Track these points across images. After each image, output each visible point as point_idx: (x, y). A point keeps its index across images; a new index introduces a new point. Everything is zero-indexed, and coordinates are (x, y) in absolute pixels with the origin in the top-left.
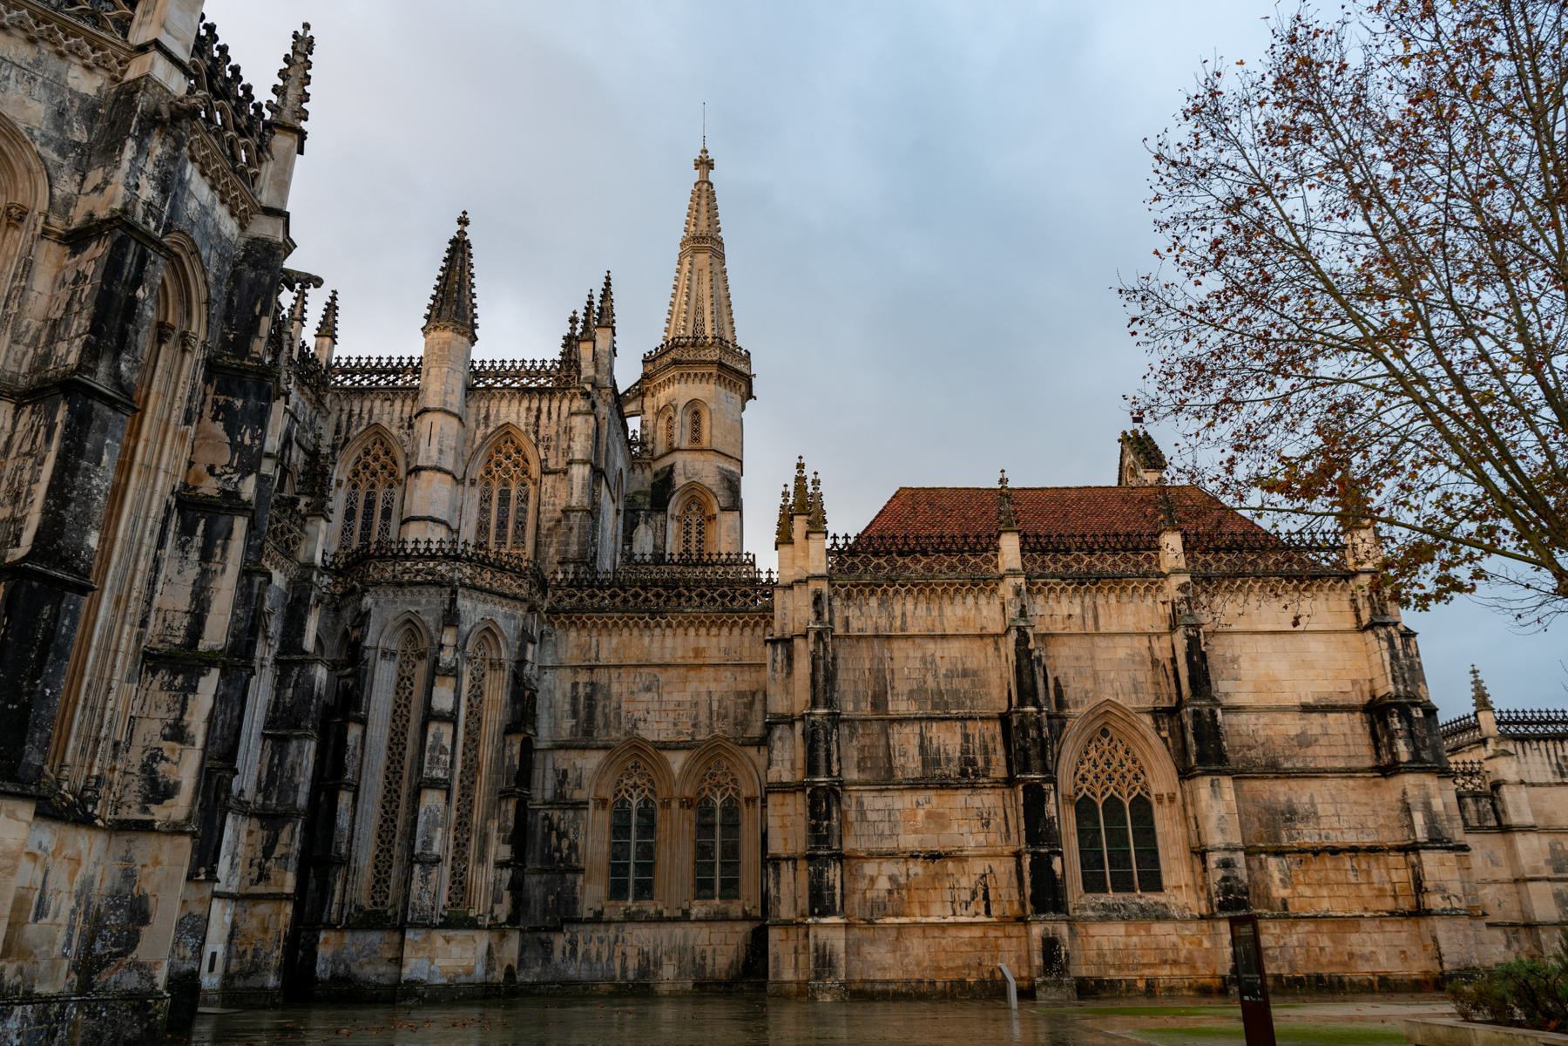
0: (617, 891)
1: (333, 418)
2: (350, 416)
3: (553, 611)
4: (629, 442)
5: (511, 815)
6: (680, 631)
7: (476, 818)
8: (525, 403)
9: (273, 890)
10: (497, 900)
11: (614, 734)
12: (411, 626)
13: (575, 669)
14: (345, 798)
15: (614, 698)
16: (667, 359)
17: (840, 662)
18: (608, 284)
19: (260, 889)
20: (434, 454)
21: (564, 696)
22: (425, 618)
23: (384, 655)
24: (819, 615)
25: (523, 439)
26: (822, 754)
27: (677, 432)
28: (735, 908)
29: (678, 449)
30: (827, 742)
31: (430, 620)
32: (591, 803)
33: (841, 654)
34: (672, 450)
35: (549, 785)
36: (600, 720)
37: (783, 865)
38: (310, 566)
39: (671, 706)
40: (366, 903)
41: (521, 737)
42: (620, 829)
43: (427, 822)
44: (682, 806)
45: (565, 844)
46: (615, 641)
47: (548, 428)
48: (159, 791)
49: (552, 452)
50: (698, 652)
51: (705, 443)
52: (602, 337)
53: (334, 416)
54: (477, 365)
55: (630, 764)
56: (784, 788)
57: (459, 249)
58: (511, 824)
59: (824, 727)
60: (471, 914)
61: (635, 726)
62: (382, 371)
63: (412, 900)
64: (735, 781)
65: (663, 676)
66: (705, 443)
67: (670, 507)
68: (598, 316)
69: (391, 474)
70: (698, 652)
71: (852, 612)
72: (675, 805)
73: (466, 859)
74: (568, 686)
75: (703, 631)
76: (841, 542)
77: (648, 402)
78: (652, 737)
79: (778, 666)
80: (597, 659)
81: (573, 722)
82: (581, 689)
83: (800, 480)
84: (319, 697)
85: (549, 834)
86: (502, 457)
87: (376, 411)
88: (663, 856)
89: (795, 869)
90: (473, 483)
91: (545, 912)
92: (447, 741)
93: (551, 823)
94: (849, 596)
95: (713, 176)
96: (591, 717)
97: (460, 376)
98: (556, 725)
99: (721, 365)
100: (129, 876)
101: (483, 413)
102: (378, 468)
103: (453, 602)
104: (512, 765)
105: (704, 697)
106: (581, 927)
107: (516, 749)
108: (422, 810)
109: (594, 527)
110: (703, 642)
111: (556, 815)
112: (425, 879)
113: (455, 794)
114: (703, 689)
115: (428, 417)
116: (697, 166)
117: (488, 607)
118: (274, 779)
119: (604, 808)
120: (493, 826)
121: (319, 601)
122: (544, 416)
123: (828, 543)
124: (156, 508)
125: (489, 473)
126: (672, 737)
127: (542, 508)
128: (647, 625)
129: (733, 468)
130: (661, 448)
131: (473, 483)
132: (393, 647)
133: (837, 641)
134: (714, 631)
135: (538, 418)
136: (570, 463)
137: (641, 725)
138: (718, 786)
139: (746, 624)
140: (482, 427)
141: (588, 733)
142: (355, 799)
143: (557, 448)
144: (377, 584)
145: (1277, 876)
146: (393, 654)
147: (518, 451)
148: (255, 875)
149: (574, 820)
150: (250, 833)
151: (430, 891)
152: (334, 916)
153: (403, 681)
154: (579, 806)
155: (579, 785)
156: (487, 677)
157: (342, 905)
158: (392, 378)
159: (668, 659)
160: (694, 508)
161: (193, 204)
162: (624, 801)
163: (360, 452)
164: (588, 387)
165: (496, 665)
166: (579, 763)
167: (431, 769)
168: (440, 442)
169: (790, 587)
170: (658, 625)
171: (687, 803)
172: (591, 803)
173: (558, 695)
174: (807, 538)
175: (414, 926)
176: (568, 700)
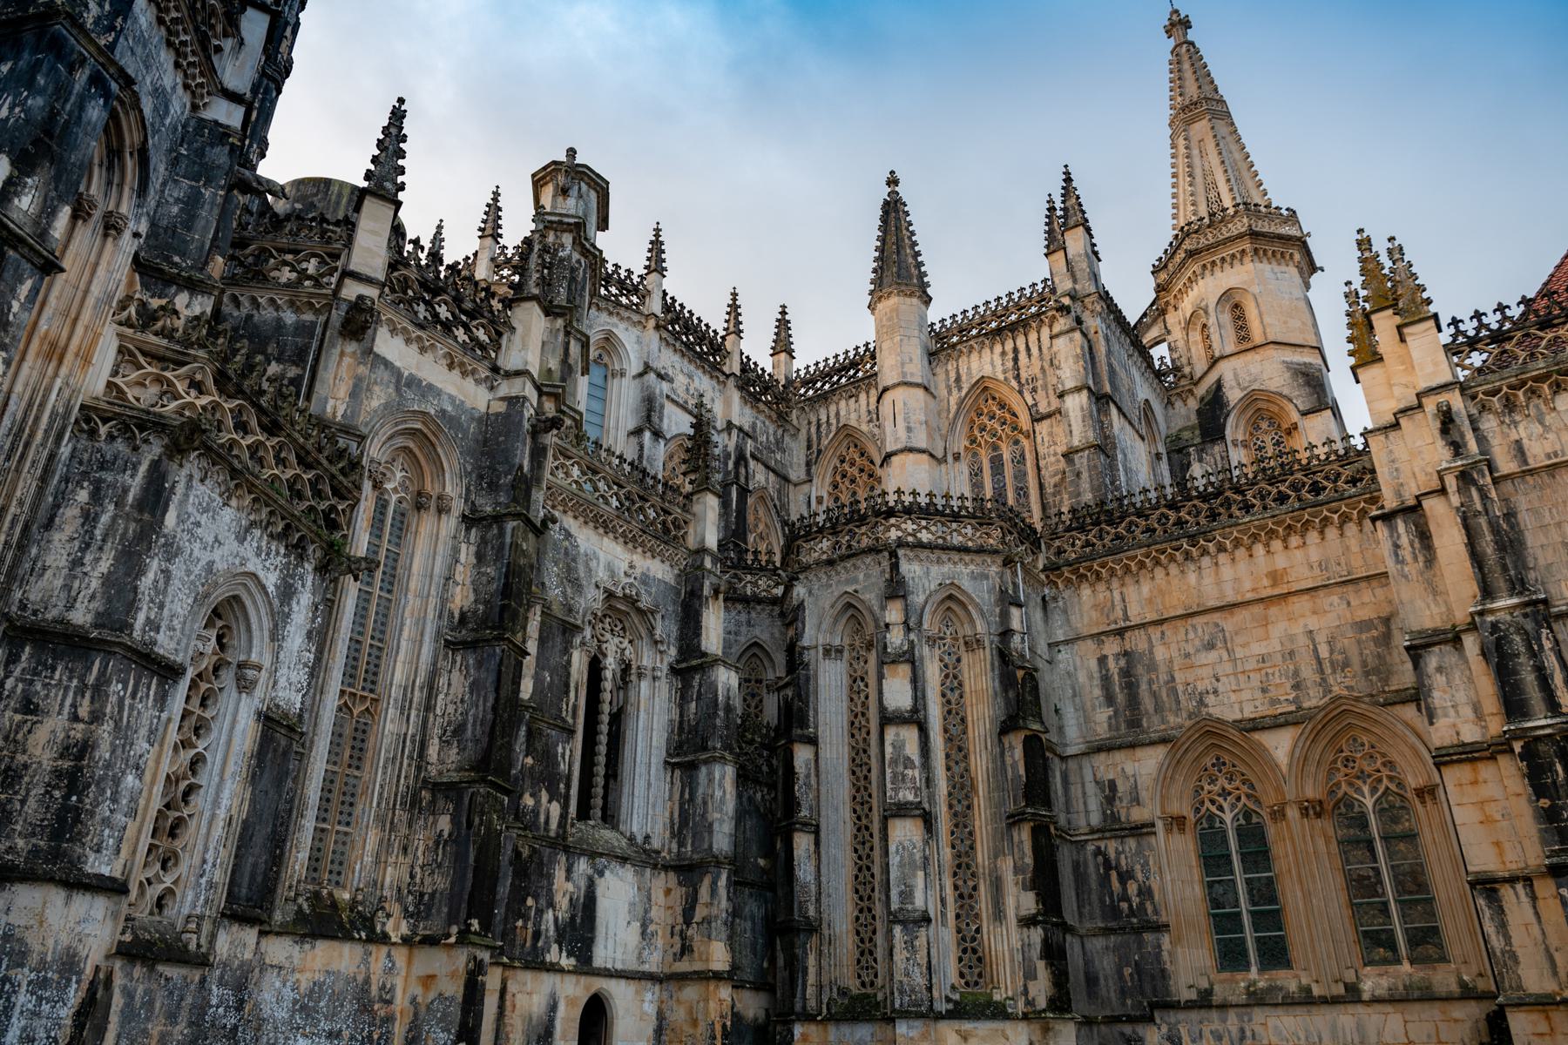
0: (1231, 957)
1: (803, 435)
2: (819, 426)
3: (1051, 568)
4: (1159, 375)
5: (1028, 847)
6: (1241, 553)
7: (982, 856)
8: (998, 348)
9: (698, 966)
10: (1030, 975)
11: (1173, 720)
12: (851, 609)
13: (1098, 637)
14: (802, 843)
15: (1163, 669)
16: (1181, 255)
17: (1525, 519)
18: (1068, 180)
19: (683, 966)
20: (902, 433)
21: (1091, 678)
22: (866, 597)
23: (827, 652)
24: (1457, 448)
25: (1004, 390)
26: (1529, 678)
27: (1215, 337)
28: (1444, 979)
29: (1222, 357)
30: (1533, 655)
31: (871, 597)
32: (1160, 825)
33: (1522, 503)
34: (1214, 362)
35: (1094, 805)
36: (1147, 703)
37: (1506, 892)
38: (702, 551)
39: (1252, 664)
40: (854, 986)
41: (1021, 735)
42: (1213, 860)
43: (901, 865)
44: (1305, 812)
45: (1132, 888)
46: (1146, 588)
47: (1030, 367)
49: (1041, 393)
50: (1275, 577)
51: (1258, 338)
52: (1075, 242)
53: (804, 431)
54: (937, 327)
55: (1208, 761)
56: (1467, 754)
58: (1029, 860)
59: (1520, 630)
60: (997, 997)
61: (1201, 703)
62: (842, 369)
63: (897, 977)
64: (1390, 764)
65: (1229, 623)
66: (1258, 338)
67: (1228, 432)
68: (1066, 218)
69: (871, 476)
70: (1275, 577)
71: (1525, 430)
72: (1293, 813)
73: (977, 916)
74: (1093, 664)
75: (1277, 545)
76: (1469, 327)
77: (1172, 318)
78: (1232, 715)
79: (1406, 553)
80: (1127, 618)
81: (1110, 711)
82: (1111, 664)
83: (1369, 266)
84: (729, 709)
85: (1107, 877)
86: (985, 419)
87: (842, 413)
88: (1292, 896)
89: (1534, 898)
90: (957, 457)
91: (1123, 992)
92: (912, 749)
93: (1107, 861)
94: (1510, 406)
96: (1133, 700)
97: (915, 341)
98: (1087, 720)
99: (1254, 235)
101: (953, 375)
102: (856, 473)
103: (895, 567)
104: (1017, 776)
105: (1303, 641)
106: (1181, 1016)
107: (1018, 753)
108: (892, 848)
109: (1112, 467)
110: (1280, 561)
111: (1112, 847)
112: (910, 945)
113: (944, 824)
114: (1298, 629)
115: (888, 397)
116: (1169, 33)
117: (946, 568)
118: (688, 820)
119: (1182, 830)
120: (1007, 866)
121: (716, 592)
122: (1023, 356)
123: (1445, 337)
125: (973, 441)
126: (1264, 709)
127: (1042, 463)
128: (1188, 556)
129: (1311, 358)
130: (1200, 366)
131: (957, 457)
132: (837, 642)
133: (1507, 487)
134: (1294, 540)
135: (1016, 360)
136: (1061, 396)
137: (1210, 700)
138: (1362, 775)
139: (1345, 519)
140: (955, 391)
141: (1134, 723)
142: (817, 843)
143: (1045, 387)
144: (806, 568)
146: (840, 651)
147: (1002, 406)
148: (678, 947)
149: (1139, 852)
150: (668, 892)
152: (812, 1003)
153: (856, 680)
154: (1141, 830)
155: (1136, 800)
156: (964, 661)
157: (820, 987)
158: (852, 372)
159: (1231, 597)
160: (1264, 425)
162: (1211, 817)
163: (836, 461)
164: (1066, 301)
165: (973, 644)
166: (1129, 770)
167: (896, 790)
168: (907, 420)
169: (1396, 426)
170: (1205, 552)
171: (1314, 810)
172: (1160, 825)
173: (1082, 677)
174: (1403, 340)
175: (905, 1014)
176: (1097, 682)
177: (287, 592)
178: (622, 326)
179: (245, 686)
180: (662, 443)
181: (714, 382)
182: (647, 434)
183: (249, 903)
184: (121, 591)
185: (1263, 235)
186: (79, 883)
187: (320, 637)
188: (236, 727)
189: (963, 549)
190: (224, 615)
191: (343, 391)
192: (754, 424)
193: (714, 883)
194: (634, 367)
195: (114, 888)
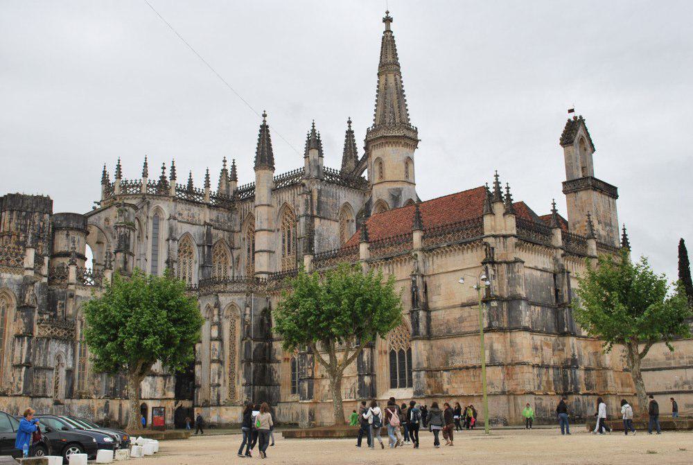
1: (239, 214)
12: (208, 308)
20: (259, 224)
48: (19, 390)
57: (264, 129)
95: (393, 26)
100: (16, 404)
103: (218, 299)
119: (288, 361)
124: (11, 340)
145: (446, 379)
151: (225, 395)
154: (278, 362)
161: (5, 281)
165: (238, 317)
175: (212, 406)
177: (67, 351)
178: (162, 202)
179: (63, 366)
180: (176, 242)
181: (200, 208)
182: (171, 241)
183: (70, 394)
184: (45, 360)
185: (389, 137)
186: (47, 397)
187: (74, 355)
188: (63, 373)
189: (236, 292)
190: (58, 358)
191: (71, 309)
192: (218, 216)
193: (169, 380)
194: (167, 217)
195: (51, 397)
